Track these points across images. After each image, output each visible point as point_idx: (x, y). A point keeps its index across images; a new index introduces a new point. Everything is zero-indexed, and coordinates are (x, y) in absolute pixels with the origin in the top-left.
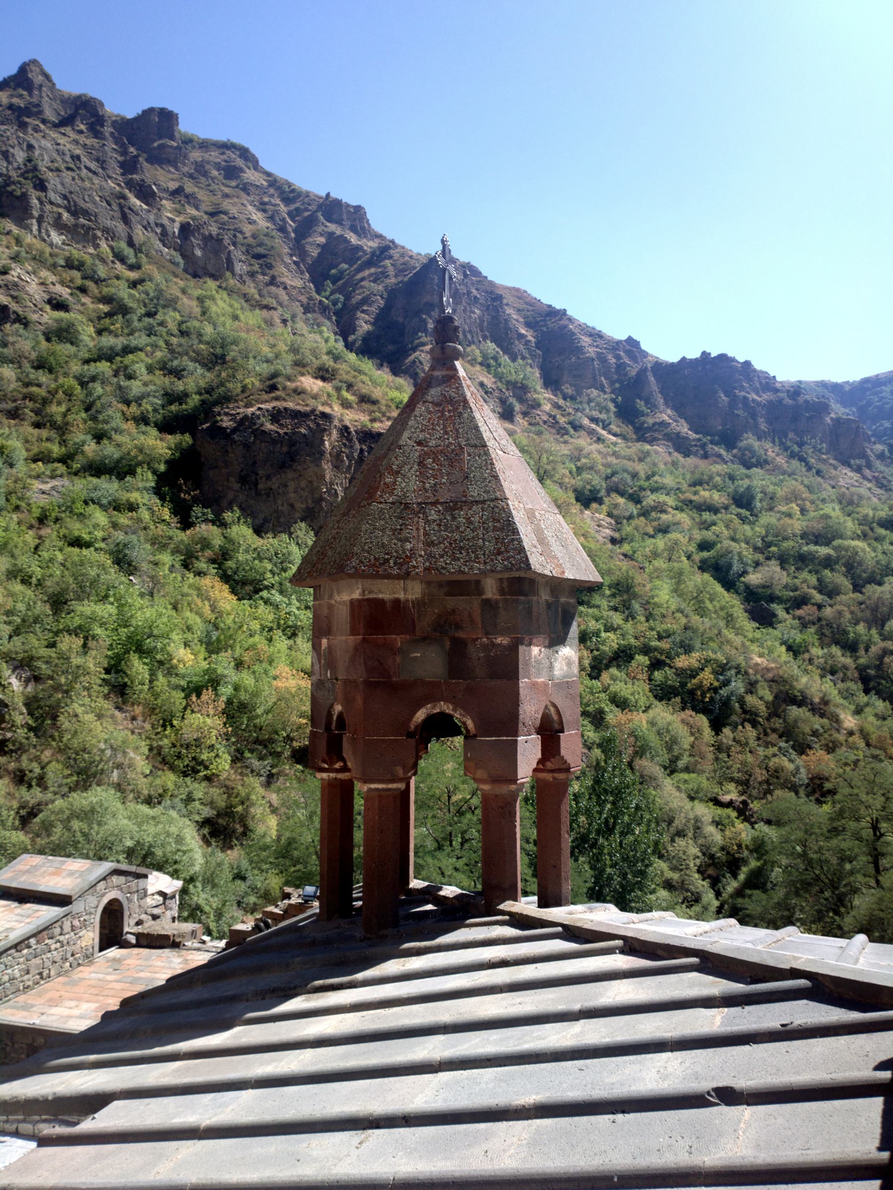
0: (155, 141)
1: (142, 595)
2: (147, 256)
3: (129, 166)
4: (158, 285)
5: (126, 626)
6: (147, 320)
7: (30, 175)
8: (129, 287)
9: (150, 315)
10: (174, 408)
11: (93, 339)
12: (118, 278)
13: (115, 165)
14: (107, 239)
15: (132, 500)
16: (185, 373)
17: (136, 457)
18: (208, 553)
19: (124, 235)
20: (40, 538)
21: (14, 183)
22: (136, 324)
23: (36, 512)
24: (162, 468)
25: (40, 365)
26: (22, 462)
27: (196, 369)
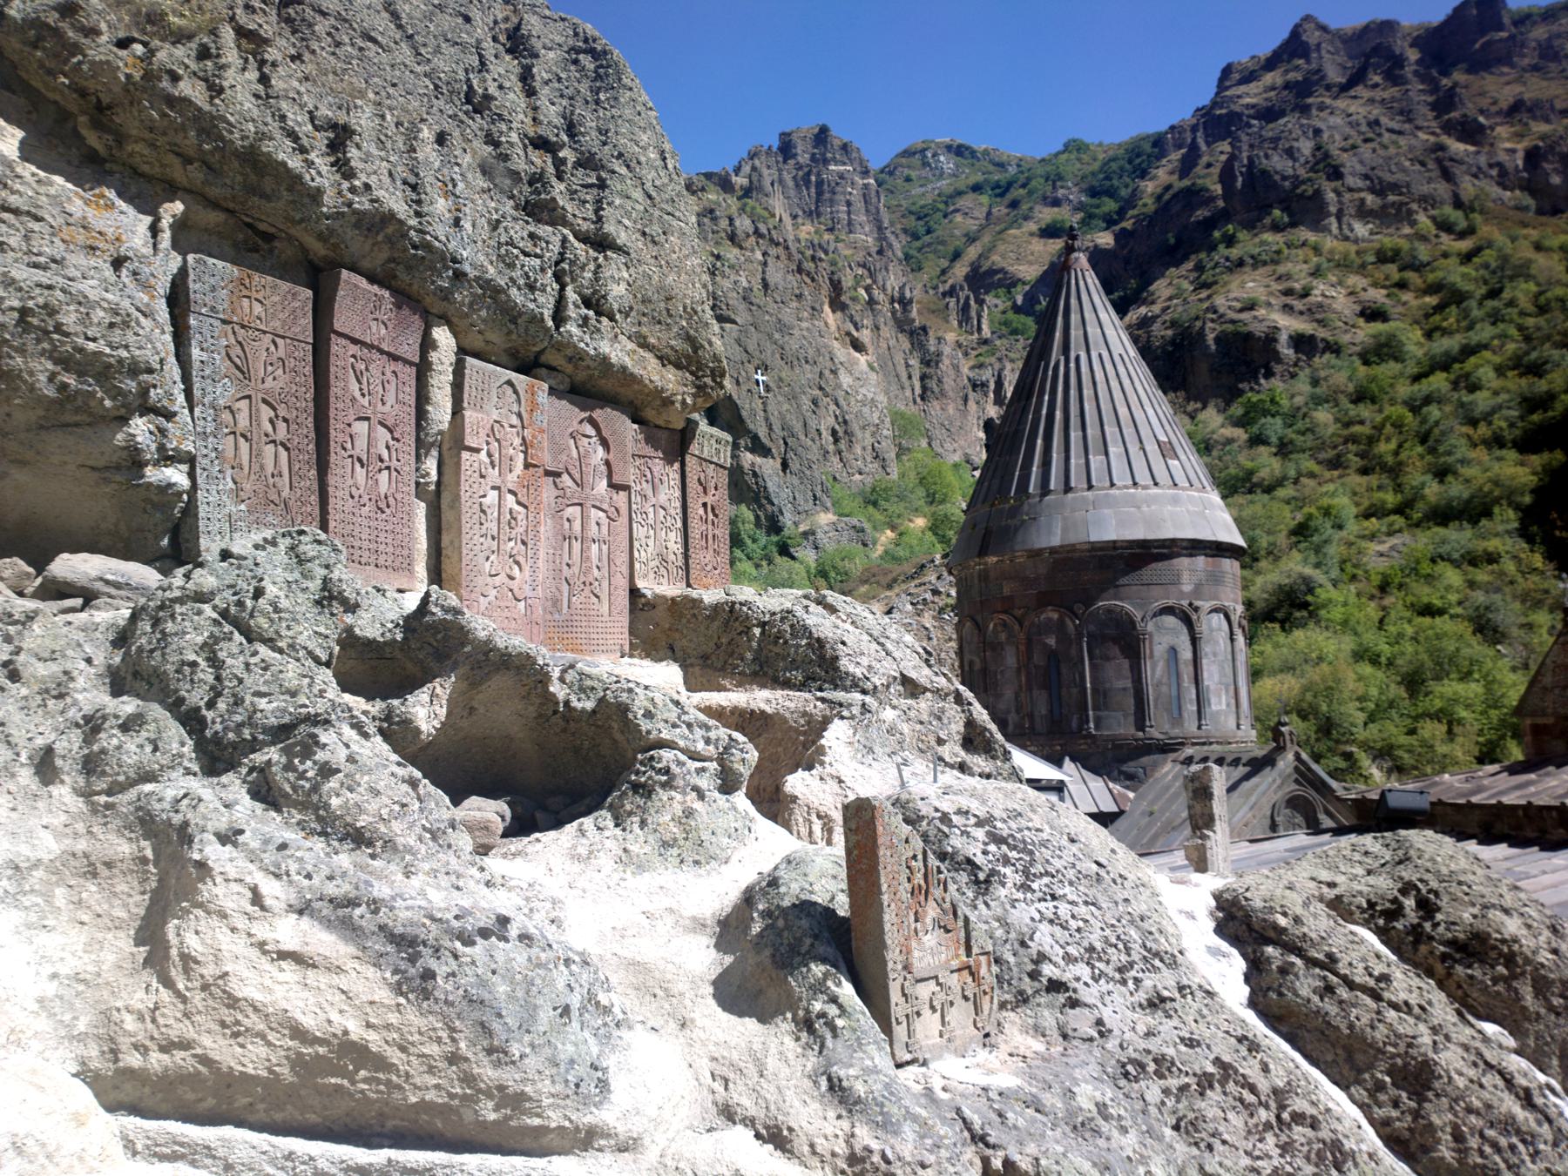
0: (1475, 41)
1: (1514, 669)
2: (1481, 213)
3: (1444, 103)
4: (1500, 250)
5: (1496, 708)
6: (1490, 304)
7: (1321, 166)
8: (1462, 263)
9: (1494, 294)
10: (1535, 417)
12: (1445, 255)
13: (1425, 110)
14: (1425, 209)
15: (1490, 549)
16: (1548, 366)
17: (1491, 492)
20: (1384, 609)
21: (1303, 182)
22: (1476, 313)
23: (1376, 580)
24: (1527, 499)
25: (1360, 397)
26: (1352, 520)
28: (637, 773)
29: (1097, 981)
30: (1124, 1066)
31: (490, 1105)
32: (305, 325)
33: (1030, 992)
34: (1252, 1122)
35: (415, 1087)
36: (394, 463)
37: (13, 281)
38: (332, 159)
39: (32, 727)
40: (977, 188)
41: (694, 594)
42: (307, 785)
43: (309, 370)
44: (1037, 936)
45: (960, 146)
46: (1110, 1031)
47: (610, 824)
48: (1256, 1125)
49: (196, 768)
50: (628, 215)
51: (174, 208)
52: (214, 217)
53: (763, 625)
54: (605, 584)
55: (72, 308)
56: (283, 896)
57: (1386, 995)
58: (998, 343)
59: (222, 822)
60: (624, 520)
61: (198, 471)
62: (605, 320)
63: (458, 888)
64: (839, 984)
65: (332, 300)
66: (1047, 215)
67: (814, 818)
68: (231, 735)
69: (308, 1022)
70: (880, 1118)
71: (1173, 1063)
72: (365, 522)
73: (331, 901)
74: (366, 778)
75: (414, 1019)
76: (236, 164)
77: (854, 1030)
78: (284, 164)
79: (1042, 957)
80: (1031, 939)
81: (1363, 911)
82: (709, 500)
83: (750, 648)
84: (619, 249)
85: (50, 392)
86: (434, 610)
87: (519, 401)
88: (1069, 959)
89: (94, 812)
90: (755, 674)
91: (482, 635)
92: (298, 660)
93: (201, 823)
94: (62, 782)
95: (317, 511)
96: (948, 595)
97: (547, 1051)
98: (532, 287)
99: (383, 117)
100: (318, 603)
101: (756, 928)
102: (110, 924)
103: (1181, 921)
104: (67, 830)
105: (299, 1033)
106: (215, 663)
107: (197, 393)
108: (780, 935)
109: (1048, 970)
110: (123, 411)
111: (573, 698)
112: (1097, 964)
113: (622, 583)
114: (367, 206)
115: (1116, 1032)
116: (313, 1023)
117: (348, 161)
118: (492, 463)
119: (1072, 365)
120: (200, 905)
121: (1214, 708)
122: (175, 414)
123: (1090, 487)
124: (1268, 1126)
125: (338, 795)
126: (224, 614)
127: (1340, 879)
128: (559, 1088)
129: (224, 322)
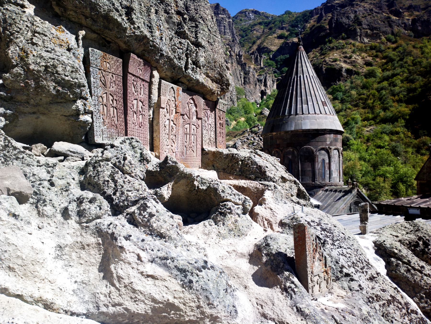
1: (402, 164)
4: (403, 47)
6: (400, 62)
8: (393, 51)
9: (401, 60)
10: (411, 95)
11: (380, 73)
12: (389, 48)
14: (384, 35)
17: (398, 115)
18: (426, 147)
19: (390, 32)
20: (368, 146)
21: (351, 26)
22: (396, 65)
23: (366, 138)
24: (408, 117)
25: (364, 87)
26: (360, 122)
27: (419, 78)
28: (221, 209)
29: (357, 273)
30: (368, 299)
31: (208, 320)
32: (120, 71)
33: (340, 277)
34: (401, 313)
35: (188, 316)
36: (143, 113)
37: (42, 57)
38: (127, 18)
39: (59, 201)
40: (260, 24)
41: (218, 149)
42: (146, 220)
43: (121, 84)
44: (340, 260)
45: (256, 11)
46: (363, 288)
47: (213, 224)
48: (402, 314)
49: (110, 213)
50: (204, 36)
51: (82, 33)
52: (94, 36)
53: (242, 161)
54: (195, 147)
55: (60, 66)
56: (147, 257)
57: (424, 272)
58: (265, 68)
59: (124, 233)
60: (200, 128)
61: (94, 116)
62: (198, 68)
63: (188, 250)
64: (293, 278)
65: (128, 63)
66: (280, 32)
67: (264, 220)
68: (121, 204)
69: (158, 297)
70: (315, 321)
71: (380, 297)
72: (136, 131)
73: (160, 258)
74: (162, 217)
75: (188, 295)
76: (101, 19)
77: (301, 292)
78: (117, 20)
79: (343, 267)
80: (339, 261)
81: (408, 245)
82: (221, 122)
83: (238, 168)
84: (203, 47)
85: (54, 92)
86: (170, 162)
87: (174, 93)
88: (349, 266)
89: (82, 228)
90: (240, 175)
91: (182, 169)
92: (137, 179)
93: (119, 233)
94: (72, 219)
95: (124, 128)
96: (251, 140)
97: (223, 303)
98: (180, 59)
99: (141, 5)
100: (140, 161)
101: (264, 259)
102: (90, 264)
103: (365, 250)
104: (75, 234)
105: (154, 300)
106: (115, 182)
107: (93, 92)
108: (272, 261)
109: (345, 270)
110: (75, 98)
111: (200, 185)
112: (356, 267)
113: (199, 147)
114: (139, 33)
115: (365, 288)
116: (158, 297)
117: (133, 18)
118: (167, 112)
119: (299, 78)
120: (122, 260)
121: (334, 176)
122: (87, 99)
123: (303, 114)
124: (405, 314)
125: (155, 223)
126: (115, 165)
127: (399, 235)
128: (226, 314)
129: (99, 69)
